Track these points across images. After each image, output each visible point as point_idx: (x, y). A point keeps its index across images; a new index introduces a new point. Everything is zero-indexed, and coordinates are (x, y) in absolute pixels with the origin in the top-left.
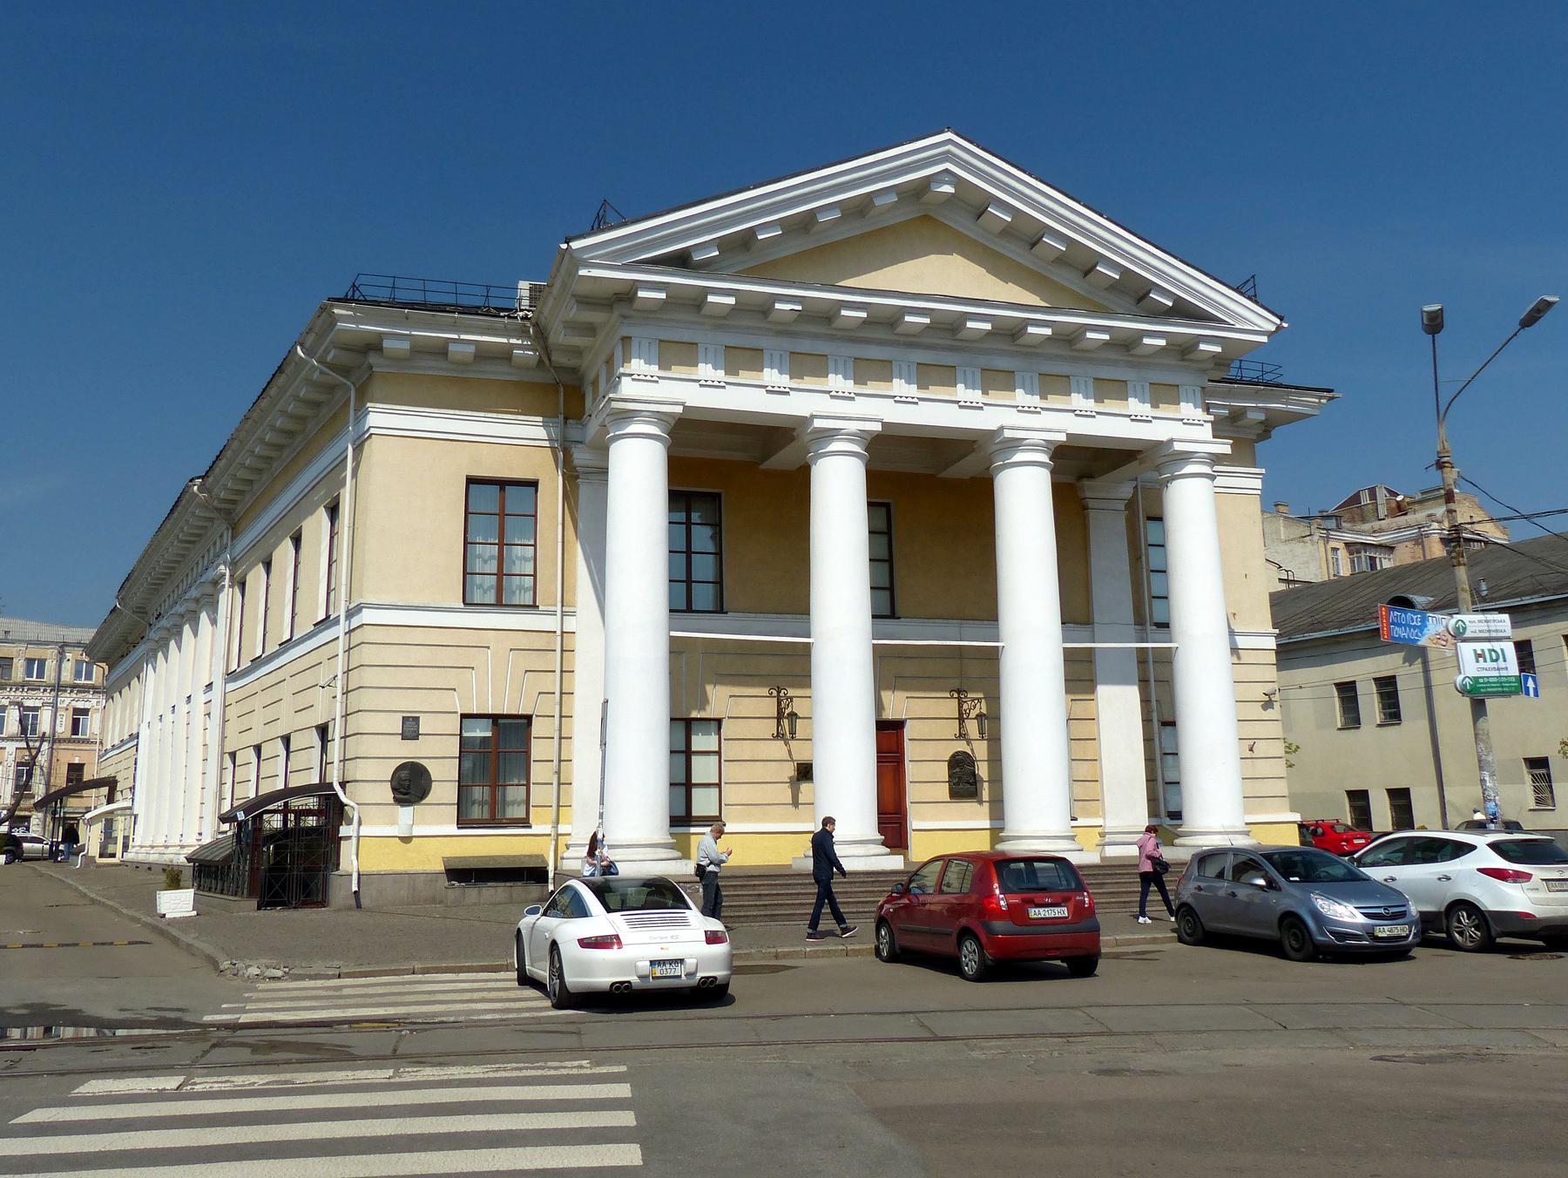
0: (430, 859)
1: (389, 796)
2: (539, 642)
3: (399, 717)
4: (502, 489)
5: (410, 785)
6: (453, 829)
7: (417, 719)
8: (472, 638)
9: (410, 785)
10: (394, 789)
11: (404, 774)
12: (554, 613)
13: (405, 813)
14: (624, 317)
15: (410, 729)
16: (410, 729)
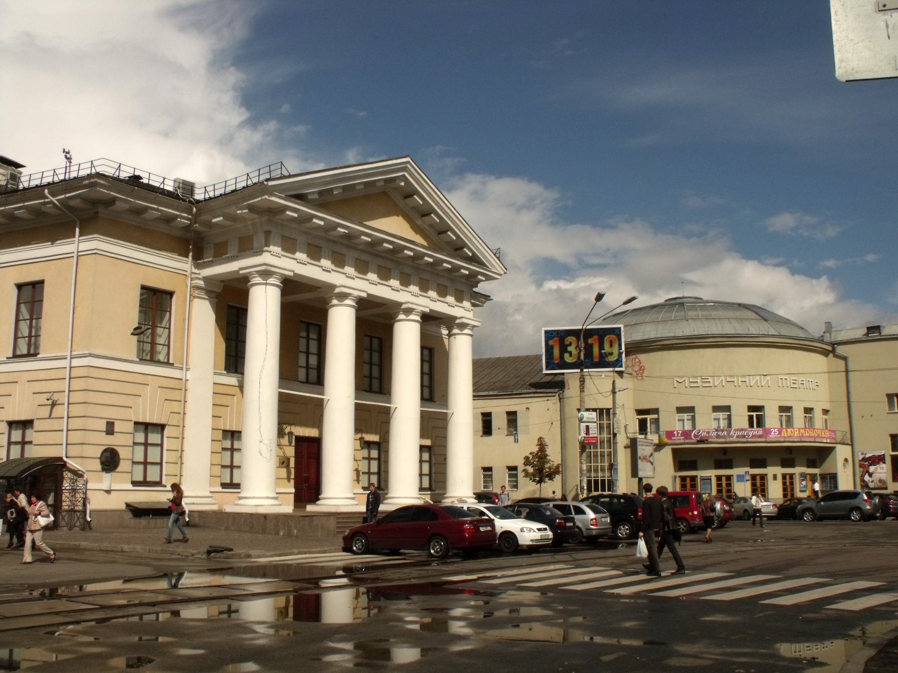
0: (117, 502)
1: (99, 467)
2: (172, 383)
3: (104, 422)
4: (155, 294)
5: (110, 461)
6: (130, 487)
7: (113, 423)
8: (140, 379)
9: (110, 461)
10: (102, 463)
11: (108, 454)
12: (181, 369)
13: (107, 476)
14: (270, 221)
15: (110, 429)
16: (110, 429)
